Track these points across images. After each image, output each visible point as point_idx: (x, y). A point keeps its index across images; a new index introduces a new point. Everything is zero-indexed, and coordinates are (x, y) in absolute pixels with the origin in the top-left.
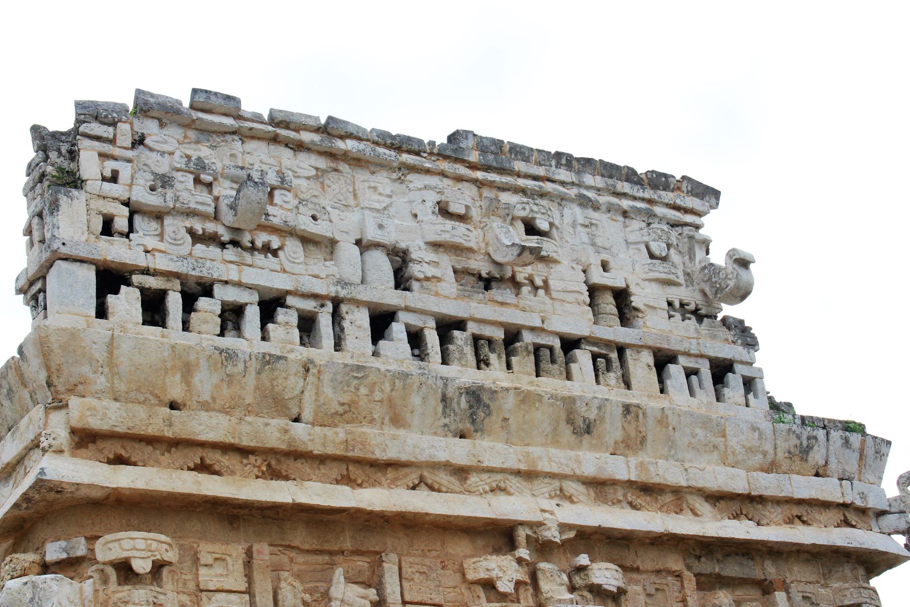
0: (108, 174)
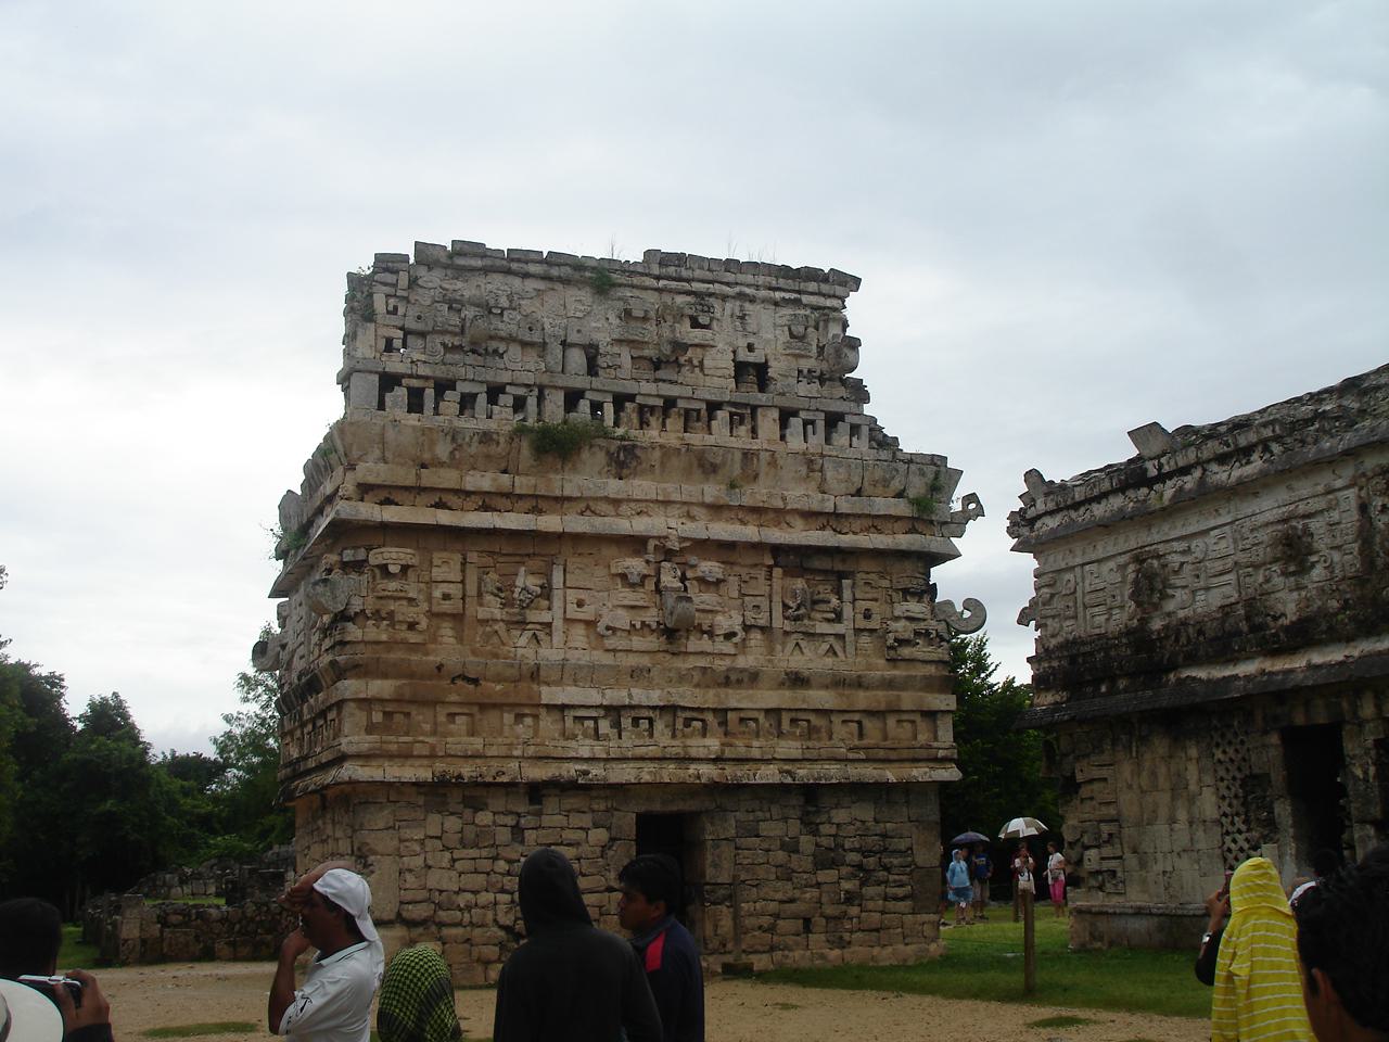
0: (391, 308)
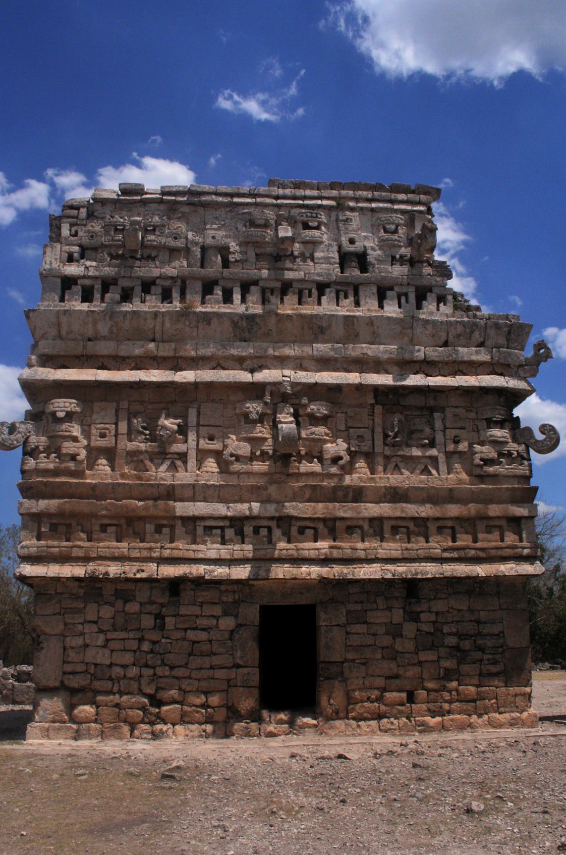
0: (73, 232)
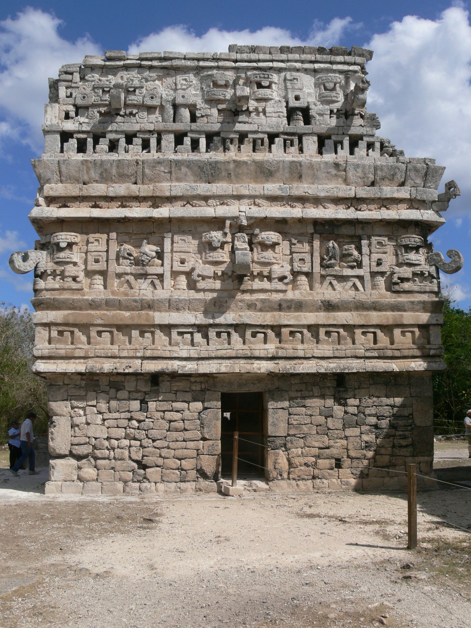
0: (69, 94)
